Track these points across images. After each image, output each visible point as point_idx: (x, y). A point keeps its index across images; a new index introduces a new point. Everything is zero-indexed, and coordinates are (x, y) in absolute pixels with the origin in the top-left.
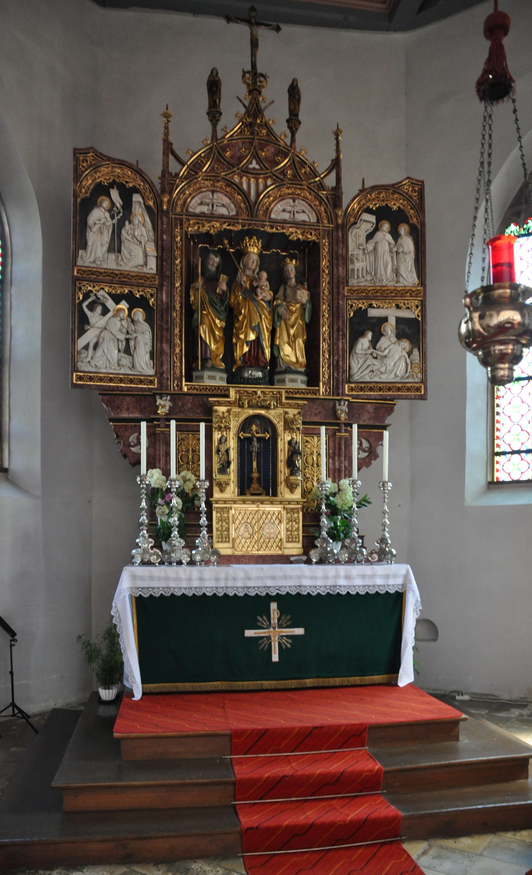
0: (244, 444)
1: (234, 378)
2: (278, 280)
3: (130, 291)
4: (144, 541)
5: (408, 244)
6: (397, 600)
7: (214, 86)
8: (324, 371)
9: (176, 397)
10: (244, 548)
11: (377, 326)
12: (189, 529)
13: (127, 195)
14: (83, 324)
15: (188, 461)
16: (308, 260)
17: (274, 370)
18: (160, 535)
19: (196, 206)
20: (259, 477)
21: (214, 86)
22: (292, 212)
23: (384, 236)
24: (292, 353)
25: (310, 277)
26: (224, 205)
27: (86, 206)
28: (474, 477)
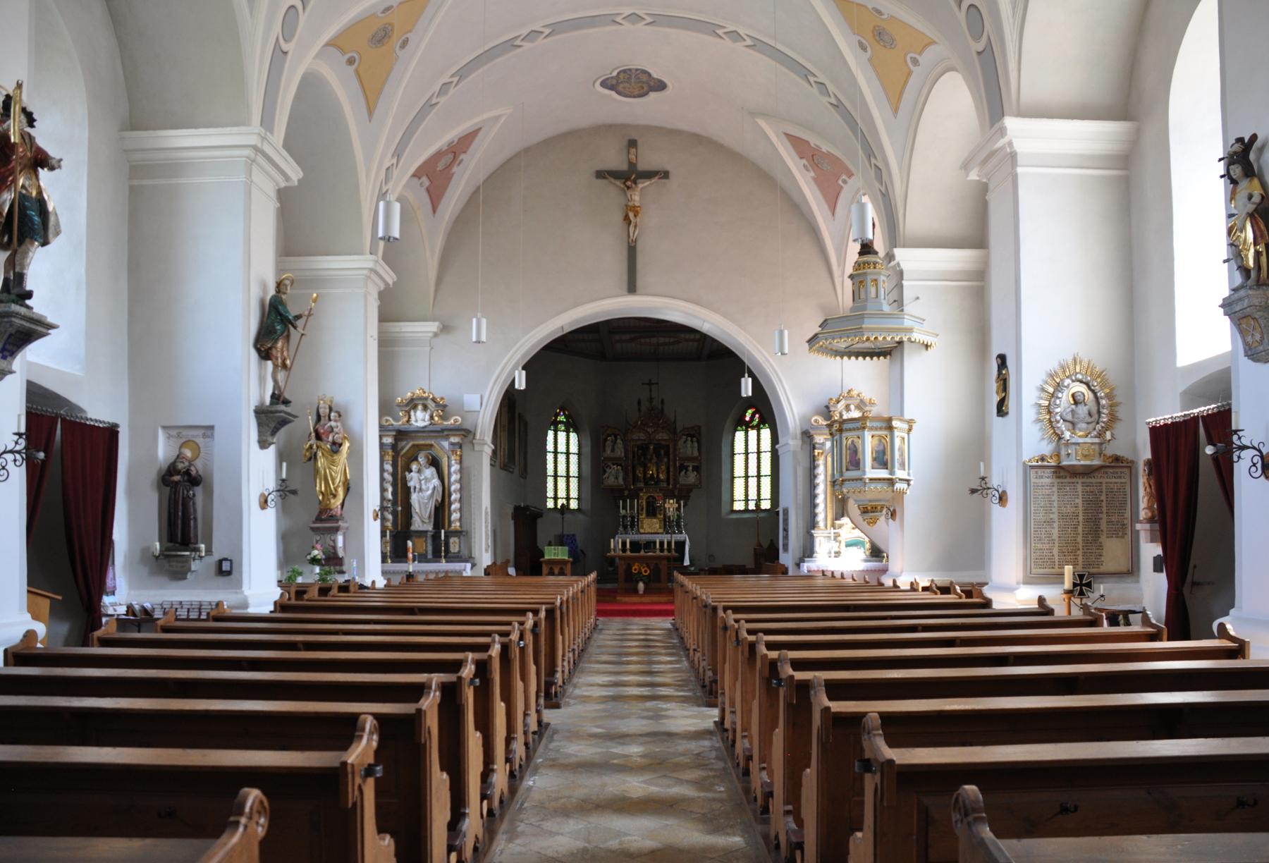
0: (648, 503)
1: (646, 484)
2: (658, 455)
3: (616, 461)
4: (621, 529)
5: (696, 444)
6: (683, 543)
7: (639, 403)
8: (671, 481)
9: (630, 490)
10: (648, 530)
11: (686, 468)
12: (632, 526)
13: (616, 436)
14: (605, 472)
15: (632, 508)
16: (663, 451)
17: (658, 480)
18: (625, 527)
19: (635, 437)
20: (652, 511)
21: (639, 403)
22: (663, 436)
23: (689, 443)
24: (662, 477)
25: (667, 454)
26: (642, 436)
27: (606, 440)
28: (725, 509)
